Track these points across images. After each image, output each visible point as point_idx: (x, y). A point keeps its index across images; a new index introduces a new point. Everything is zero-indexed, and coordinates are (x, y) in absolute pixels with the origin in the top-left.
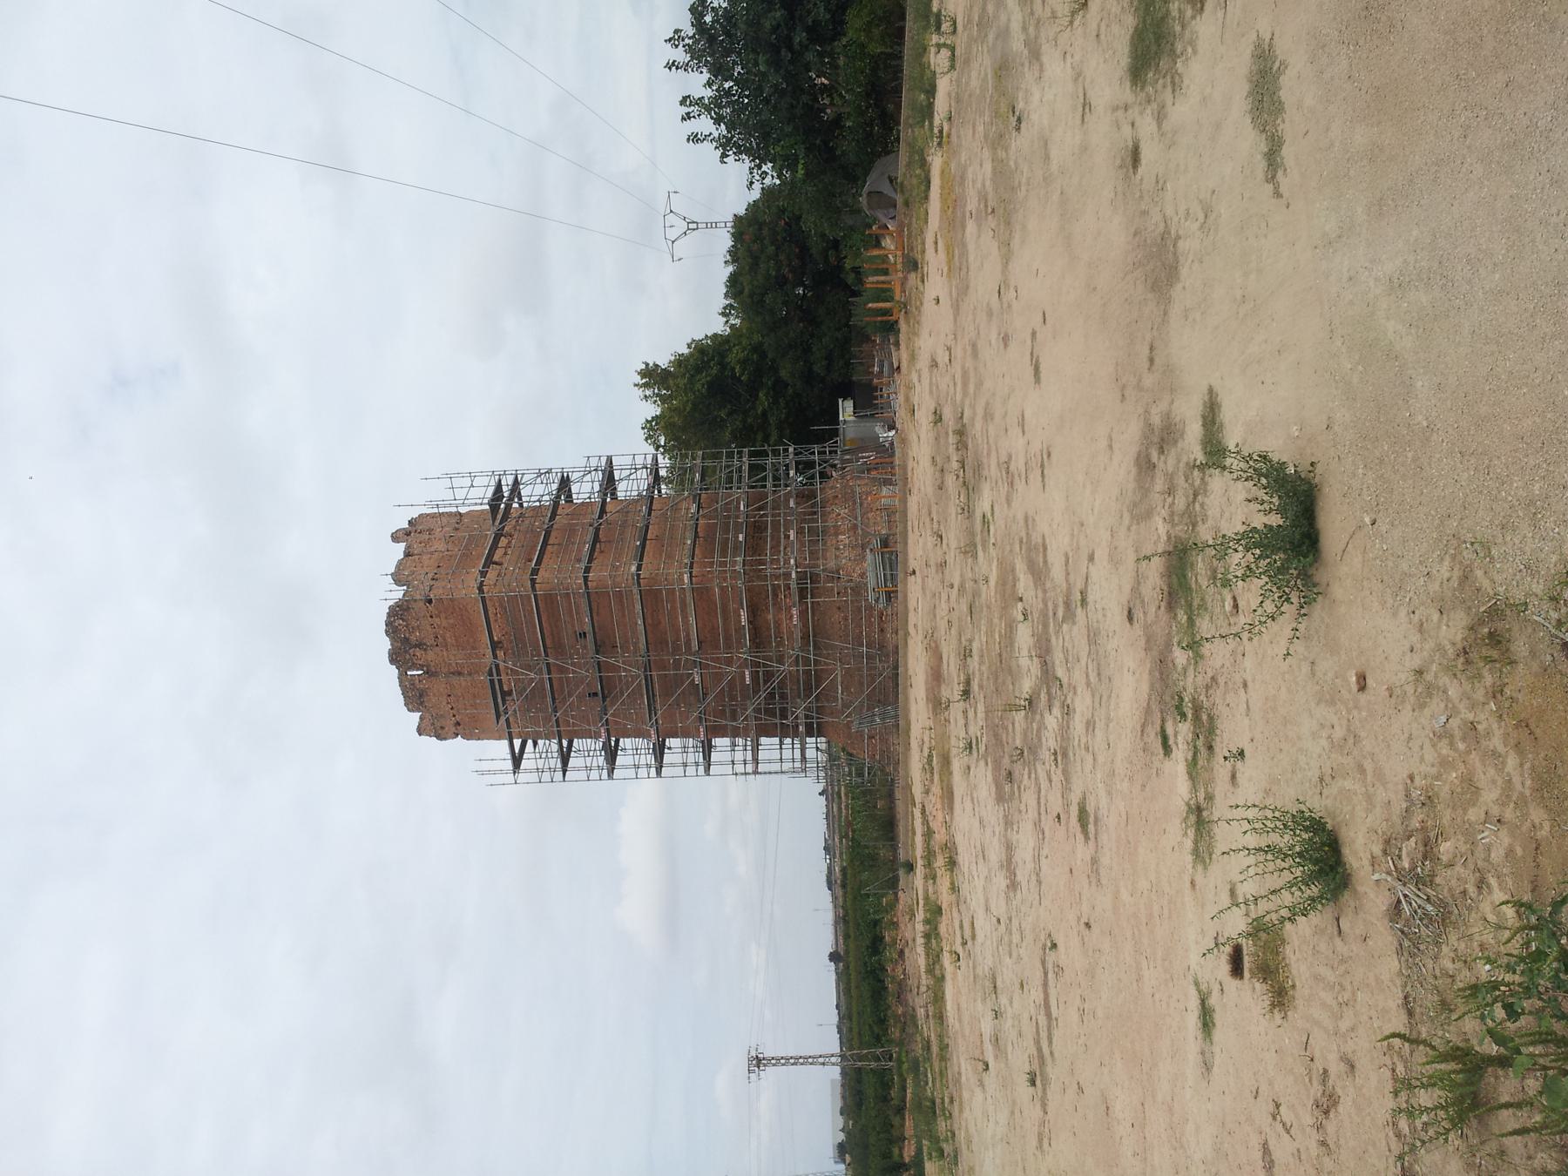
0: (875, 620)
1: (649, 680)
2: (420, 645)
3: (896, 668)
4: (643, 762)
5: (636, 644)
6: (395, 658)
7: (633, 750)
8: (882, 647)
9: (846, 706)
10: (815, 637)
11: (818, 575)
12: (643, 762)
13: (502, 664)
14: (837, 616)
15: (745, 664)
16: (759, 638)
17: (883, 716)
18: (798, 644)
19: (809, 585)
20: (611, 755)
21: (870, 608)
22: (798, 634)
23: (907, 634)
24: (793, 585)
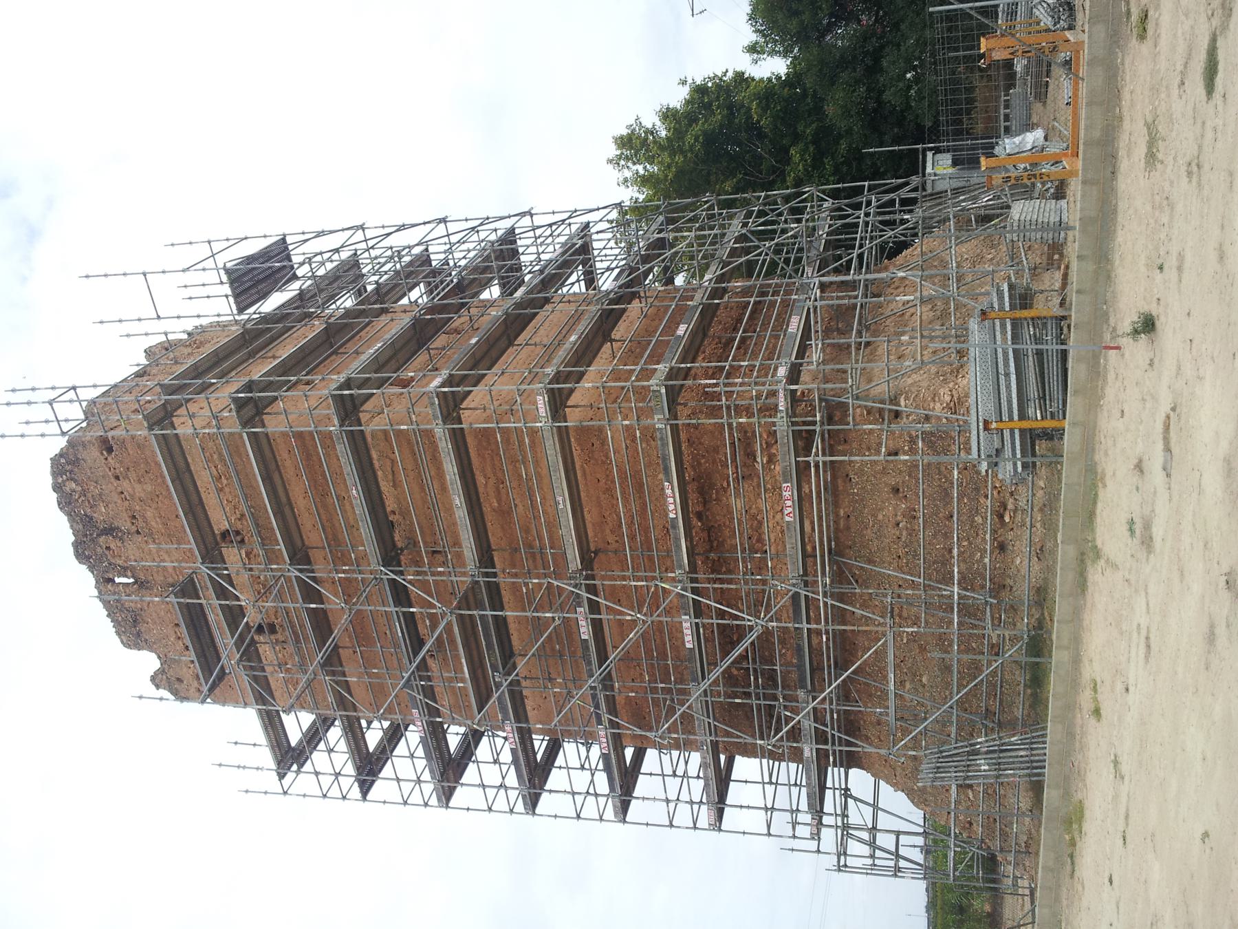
0: (987, 521)
1: (467, 625)
2: (110, 531)
3: (1038, 645)
4: (782, 802)
5: (459, 556)
6: (83, 551)
7: (669, 774)
8: (999, 588)
9: (908, 717)
10: (842, 555)
11: (844, 407)
12: (782, 802)
13: (503, 580)
14: (891, 509)
15: (680, 606)
16: (711, 547)
17: (998, 754)
18: (793, 568)
19: (825, 427)
20: (624, 781)
21: (974, 485)
22: (793, 544)
23: (1088, 554)
24: (781, 423)
